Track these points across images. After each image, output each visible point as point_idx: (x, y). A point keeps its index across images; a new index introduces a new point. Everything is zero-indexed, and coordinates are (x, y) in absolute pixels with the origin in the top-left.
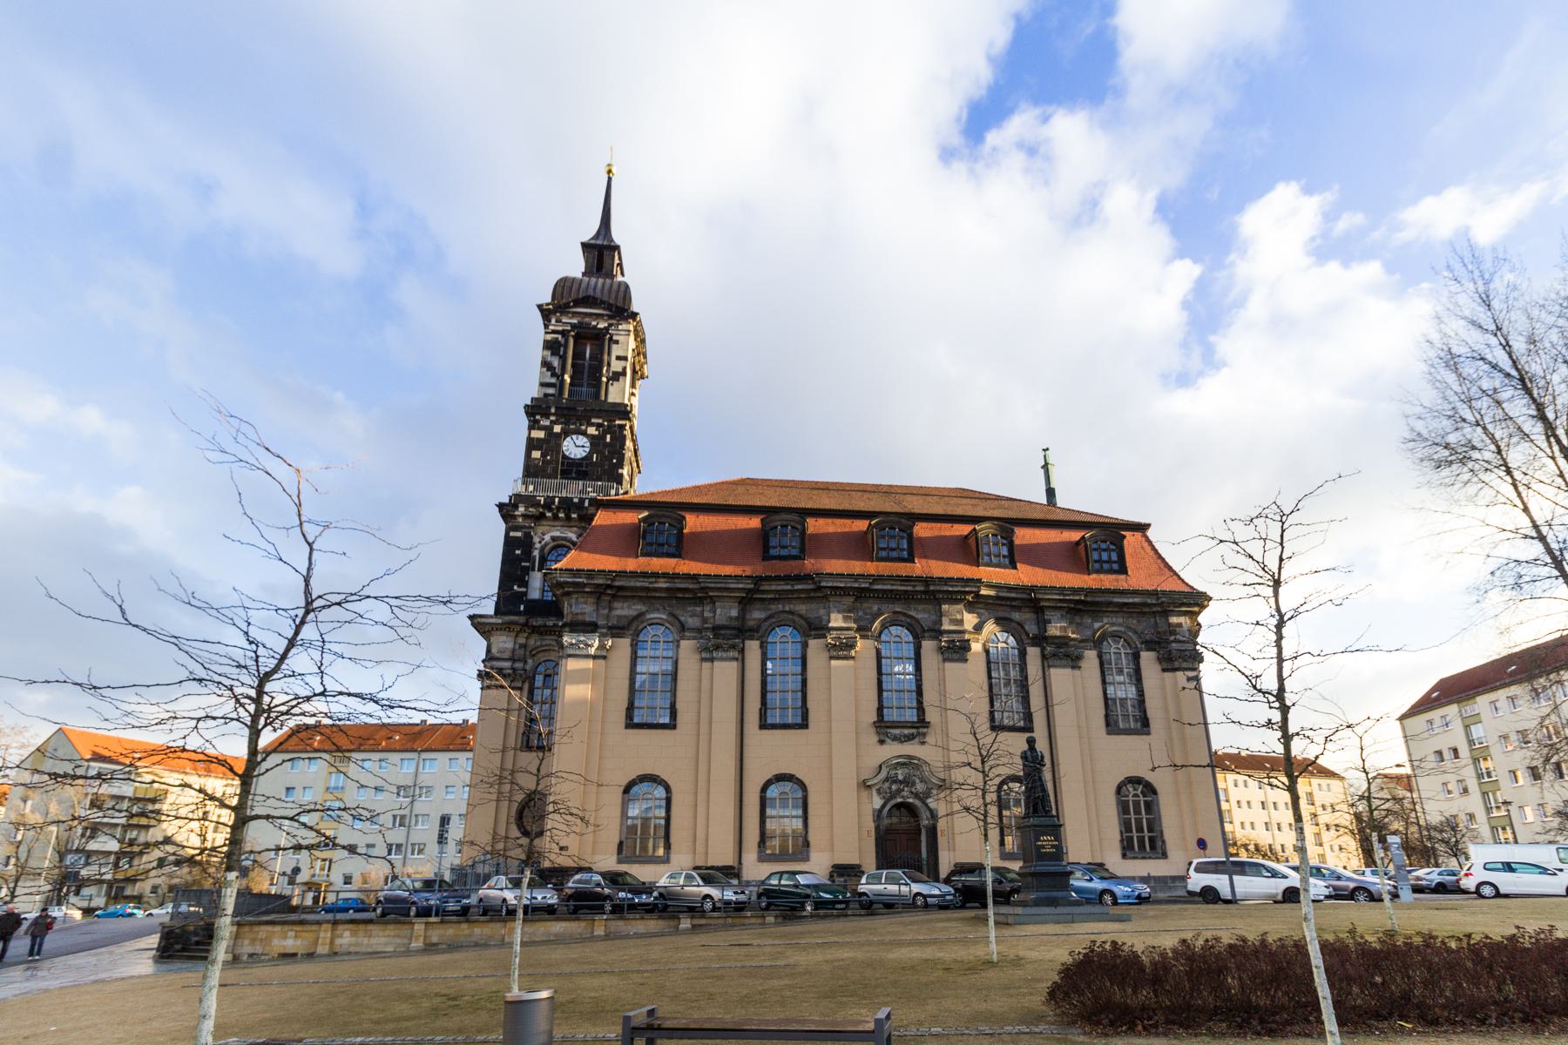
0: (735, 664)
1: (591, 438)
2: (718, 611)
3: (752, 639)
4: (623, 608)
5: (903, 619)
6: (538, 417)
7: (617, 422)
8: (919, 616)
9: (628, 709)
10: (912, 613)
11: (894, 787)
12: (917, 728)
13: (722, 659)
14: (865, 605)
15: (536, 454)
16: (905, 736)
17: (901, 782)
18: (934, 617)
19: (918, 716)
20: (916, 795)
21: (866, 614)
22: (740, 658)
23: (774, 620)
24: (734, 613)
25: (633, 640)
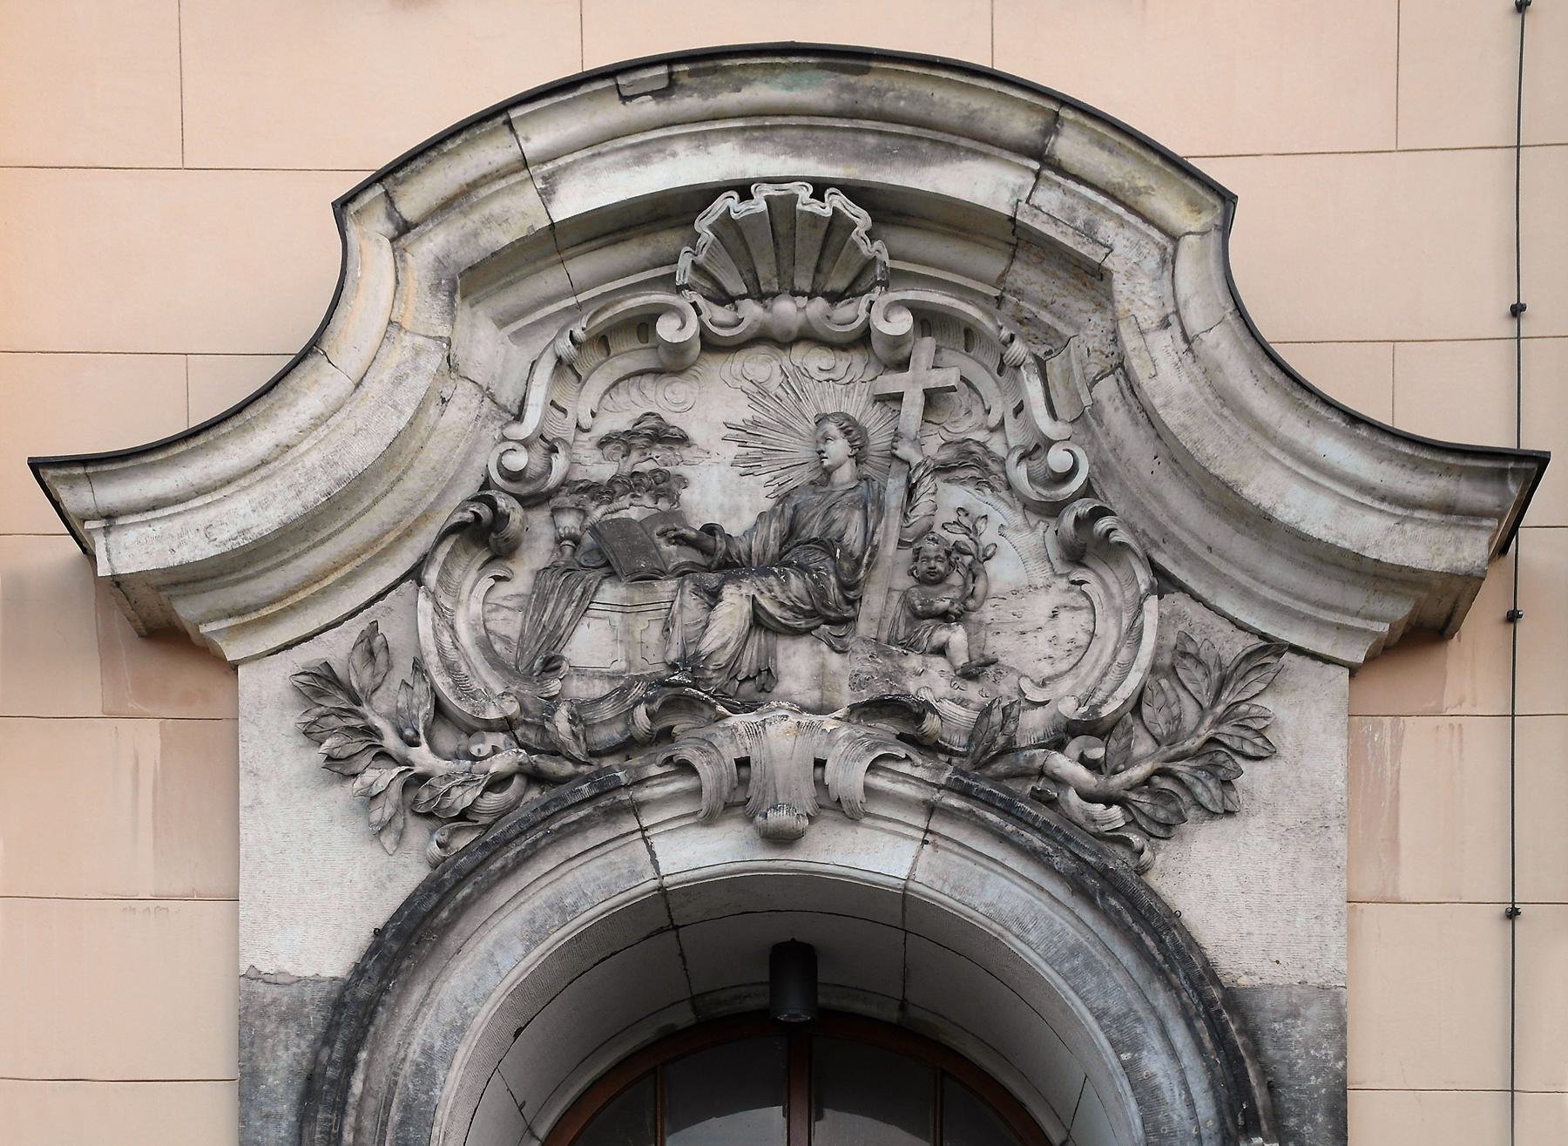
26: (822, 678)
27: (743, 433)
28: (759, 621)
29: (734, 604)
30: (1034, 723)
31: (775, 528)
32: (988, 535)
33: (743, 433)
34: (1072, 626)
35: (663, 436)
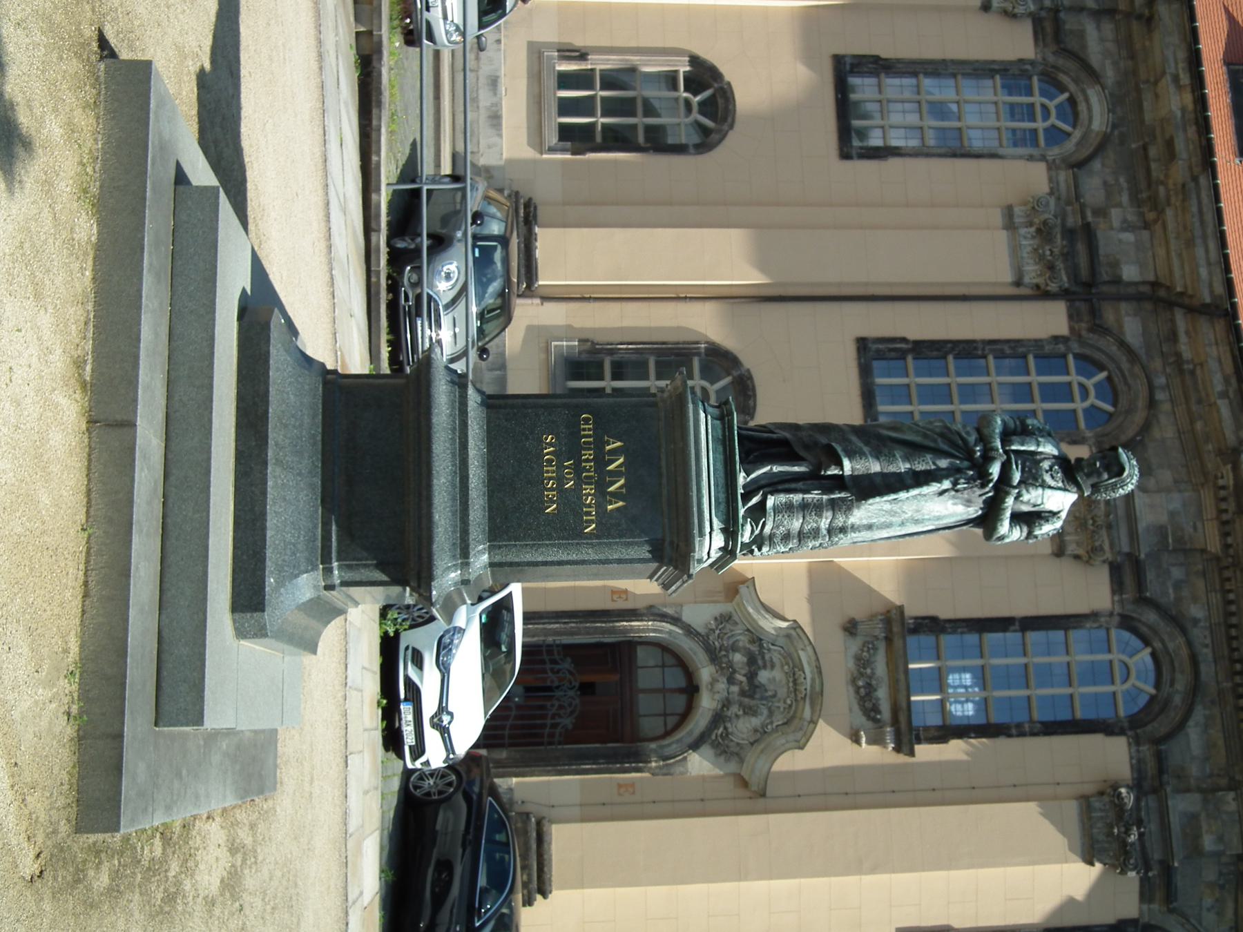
0: (1008, 277)
2: (1129, 237)
3: (1071, 317)
4: (1102, 40)
5: (1180, 685)
8: (1194, 735)
9: (876, 59)
10: (1199, 714)
11: (738, 658)
12: (895, 722)
13: (1015, 249)
14: (1200, 584)
16: (870, 688)
17: (751, 676)
18: (1194, 770)
19: (926, 728)
20: (718, 718)
21: (1178, 586)
22: (1022, 291)
23: (1125, 366)
24: (1130, 273)
25: (1032, 63)
26: (733, 693)
27: (774, 679)
28: (741, 682)
29: (743, 679)
30: (729, 725)
31: (757, 683)
32: (759, 717)
33: (774, 679)
34: (745, 730)
35: (773, 667)
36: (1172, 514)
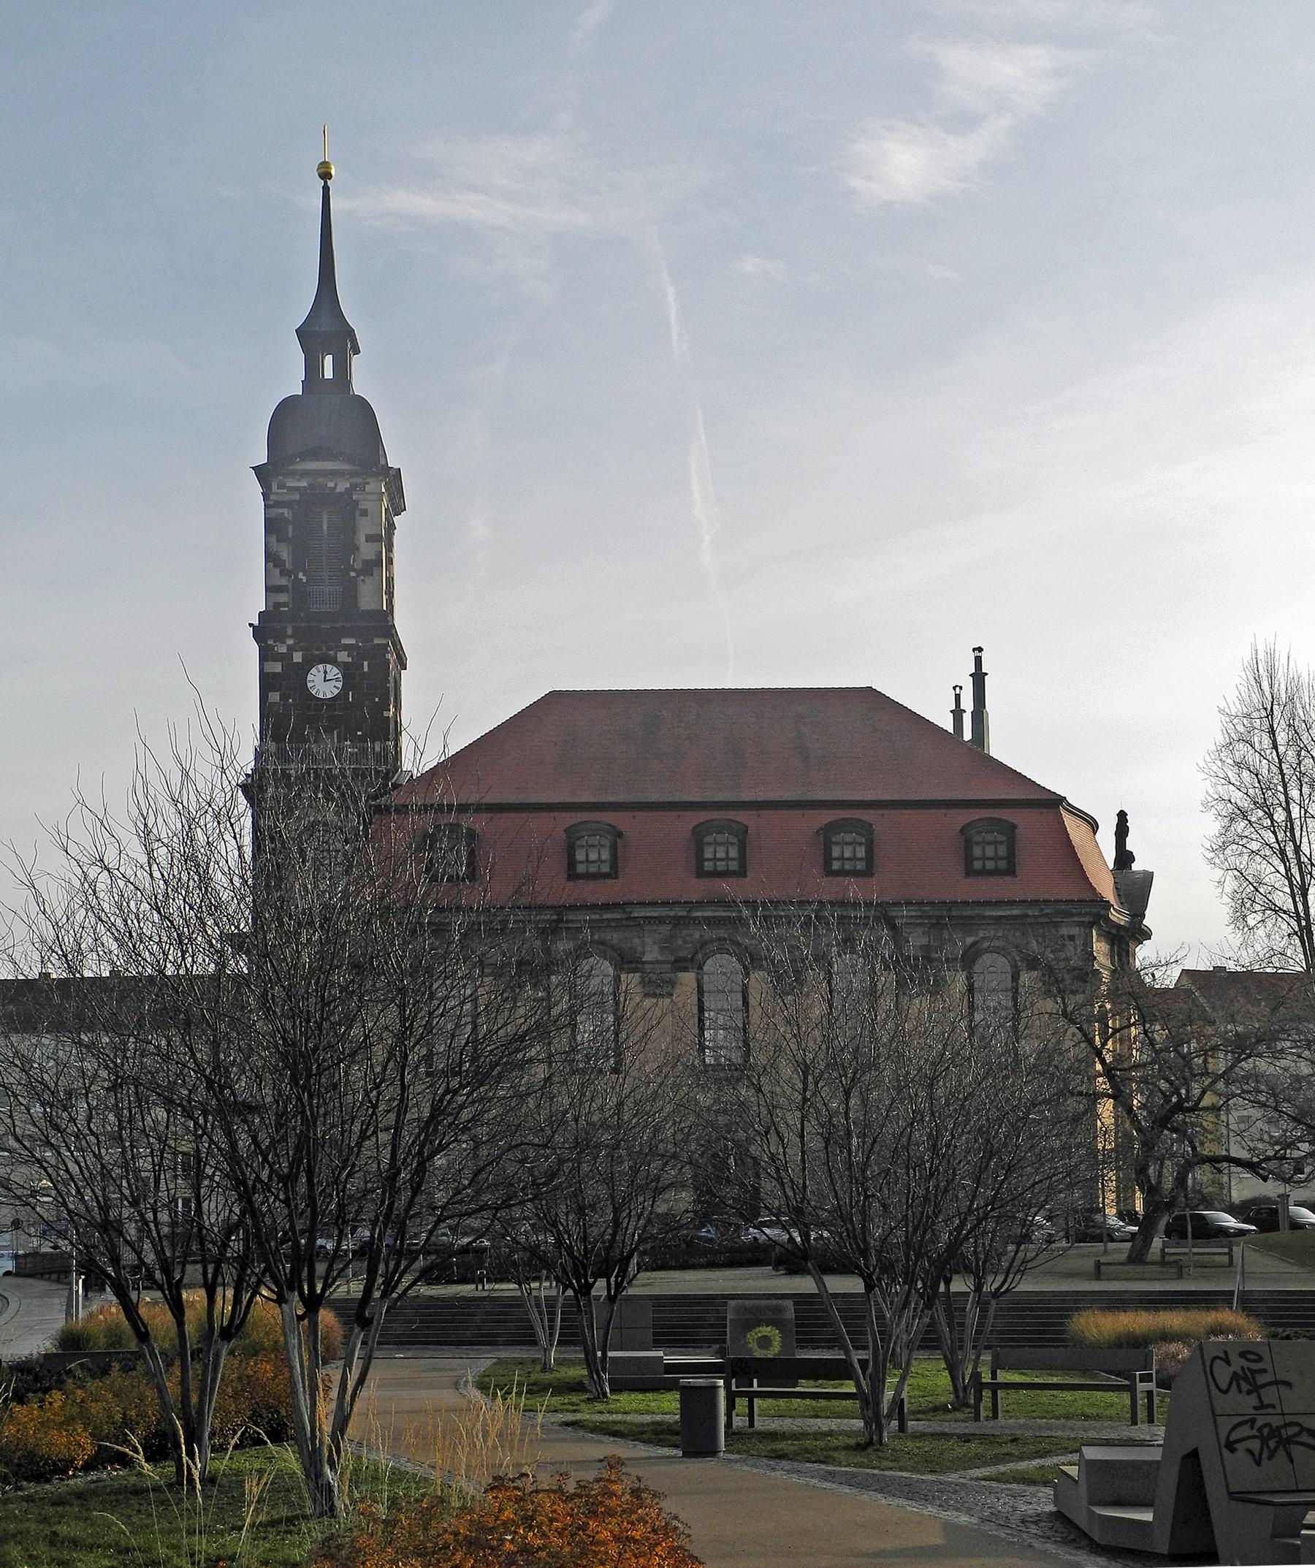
1: (345, 669)
6: (271, 642)
7: (377, 641)
14: (685, 932)
15: (275, 697)
21: (685, 942)
36: (655, 943)
